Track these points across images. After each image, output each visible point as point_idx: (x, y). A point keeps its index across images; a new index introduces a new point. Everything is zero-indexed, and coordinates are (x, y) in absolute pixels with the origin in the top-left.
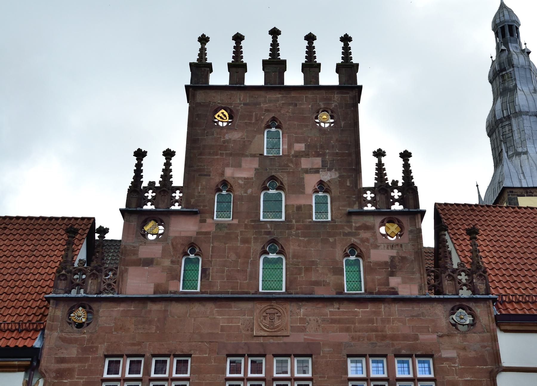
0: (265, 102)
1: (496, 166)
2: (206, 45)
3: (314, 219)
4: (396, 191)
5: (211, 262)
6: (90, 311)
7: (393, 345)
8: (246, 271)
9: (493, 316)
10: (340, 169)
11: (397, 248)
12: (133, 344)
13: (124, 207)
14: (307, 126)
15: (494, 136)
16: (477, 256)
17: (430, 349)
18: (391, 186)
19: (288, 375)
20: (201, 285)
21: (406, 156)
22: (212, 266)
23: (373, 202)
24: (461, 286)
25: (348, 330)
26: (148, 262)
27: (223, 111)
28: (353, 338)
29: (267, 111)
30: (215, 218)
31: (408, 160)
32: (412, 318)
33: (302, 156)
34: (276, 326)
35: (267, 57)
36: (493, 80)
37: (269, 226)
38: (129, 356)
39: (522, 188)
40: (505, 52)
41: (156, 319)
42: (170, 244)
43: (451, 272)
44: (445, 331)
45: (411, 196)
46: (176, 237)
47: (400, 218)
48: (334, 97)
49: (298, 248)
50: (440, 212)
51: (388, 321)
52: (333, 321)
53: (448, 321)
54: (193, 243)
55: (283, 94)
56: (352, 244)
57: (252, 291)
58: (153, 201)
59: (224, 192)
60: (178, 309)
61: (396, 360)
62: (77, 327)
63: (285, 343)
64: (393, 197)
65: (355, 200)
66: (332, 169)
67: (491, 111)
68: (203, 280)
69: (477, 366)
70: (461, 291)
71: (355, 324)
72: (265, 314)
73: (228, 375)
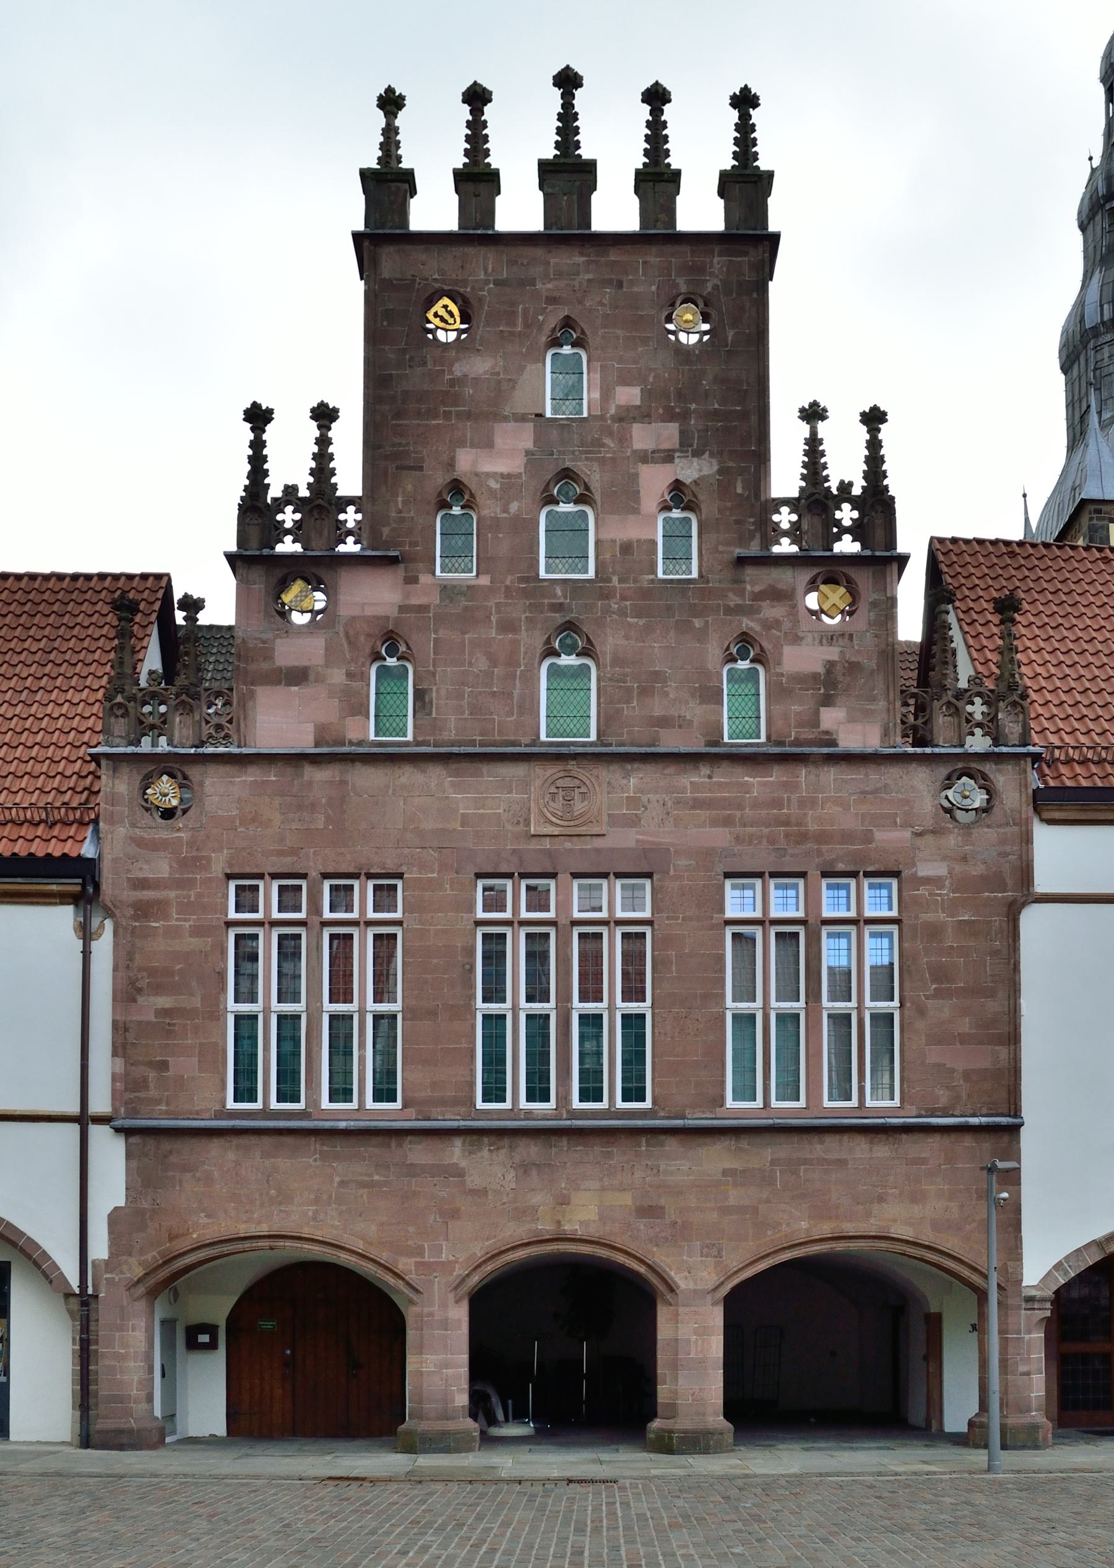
0: (546, 277)
1: (1072, 447)
2: (396, 117)
3: (660, 575)
4: (846, 507)
5: (434, 674)
6: (184, 784)
7: (819, 853)
8: (510, 695)
9: (1030, 791)
10: (720, 453)
11: (841, 642)
12: (281, 853)
13: (233, 547)
14: (645, 341)
15: (1075, 371)
16: (1012, 660)
17: (896, 861)
18: (836, 496)
19: (603, 915)
20: (415, 727)
21: (874, 418)
22: (436, 684)
23: (795, 533)
24: (971, 727)
25: (727, 822)
26: (297, 676)
27: (446, 301)
28: (737, 838)
29: (553, 300)
30: (438, 572)
31: (879, 430)
32: (863, 796)
33: (634, 420)
34: (576, 814)
35: (550, 153)
36: (1089, 223)
37: (559, 592)
38: (274, 876)
41: (324, 801)
42: (342, 634)
43: (953, 696)
44: (929, 823)
45: (879, 521)
46: (353, 618)
47: (853, 572)
48: (712, 263)
49: (622, 642)
50: (941, 558)
51: (813, 802)
52: (697, 804)
53: (936, 802)
54: (392, 631)
55: (589, 255)
56: (744, 633)
57: (525, 740)
58: (297, 533)
59: (456, 510)
60: (367, 778)
61: (824, 882)
62: (163, 817)
63: (598, 851)
65: (752, 528)
66: (703, 453)
67: (1074, 306)
68: (419, 715)
70: (969, 740)
71: (743, 809)
72: (553, 790)
73: (481, 915)
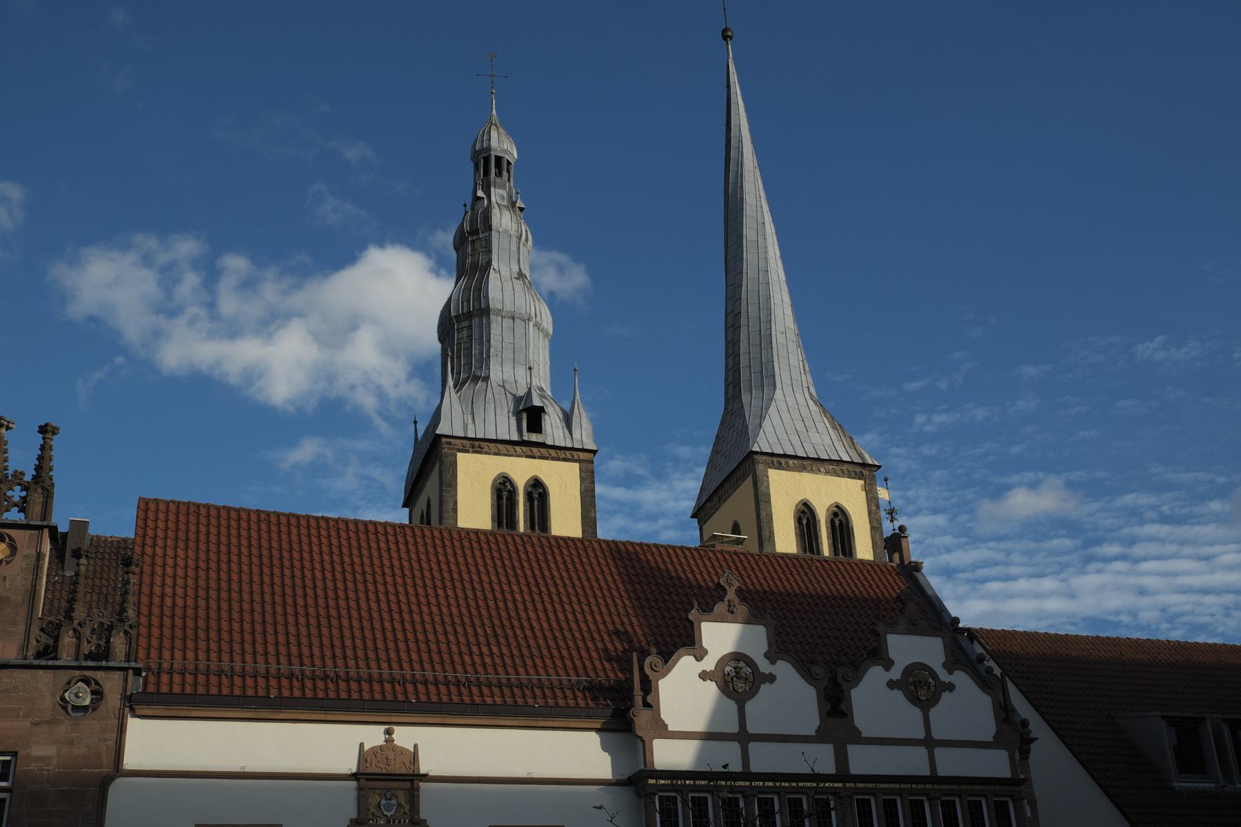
39: (465, 438)
40: (482, 200)
53: (54, 700)
64: (8, 499)
69: (86, 770)
